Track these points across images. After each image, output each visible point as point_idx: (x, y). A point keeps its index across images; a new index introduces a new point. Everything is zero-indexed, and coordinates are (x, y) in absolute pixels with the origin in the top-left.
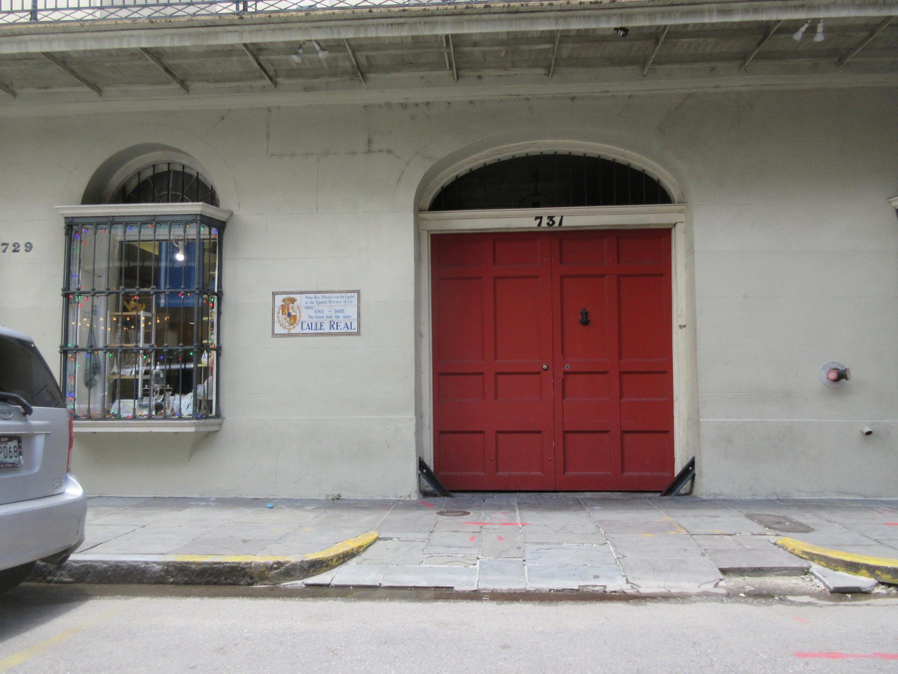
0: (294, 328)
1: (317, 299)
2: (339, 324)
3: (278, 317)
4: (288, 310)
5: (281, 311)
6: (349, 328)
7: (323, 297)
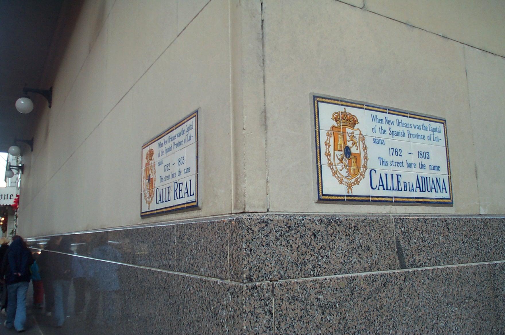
0: (357, 182)
1: (391, 126)
3: (328, 155)
7: (399, 124)
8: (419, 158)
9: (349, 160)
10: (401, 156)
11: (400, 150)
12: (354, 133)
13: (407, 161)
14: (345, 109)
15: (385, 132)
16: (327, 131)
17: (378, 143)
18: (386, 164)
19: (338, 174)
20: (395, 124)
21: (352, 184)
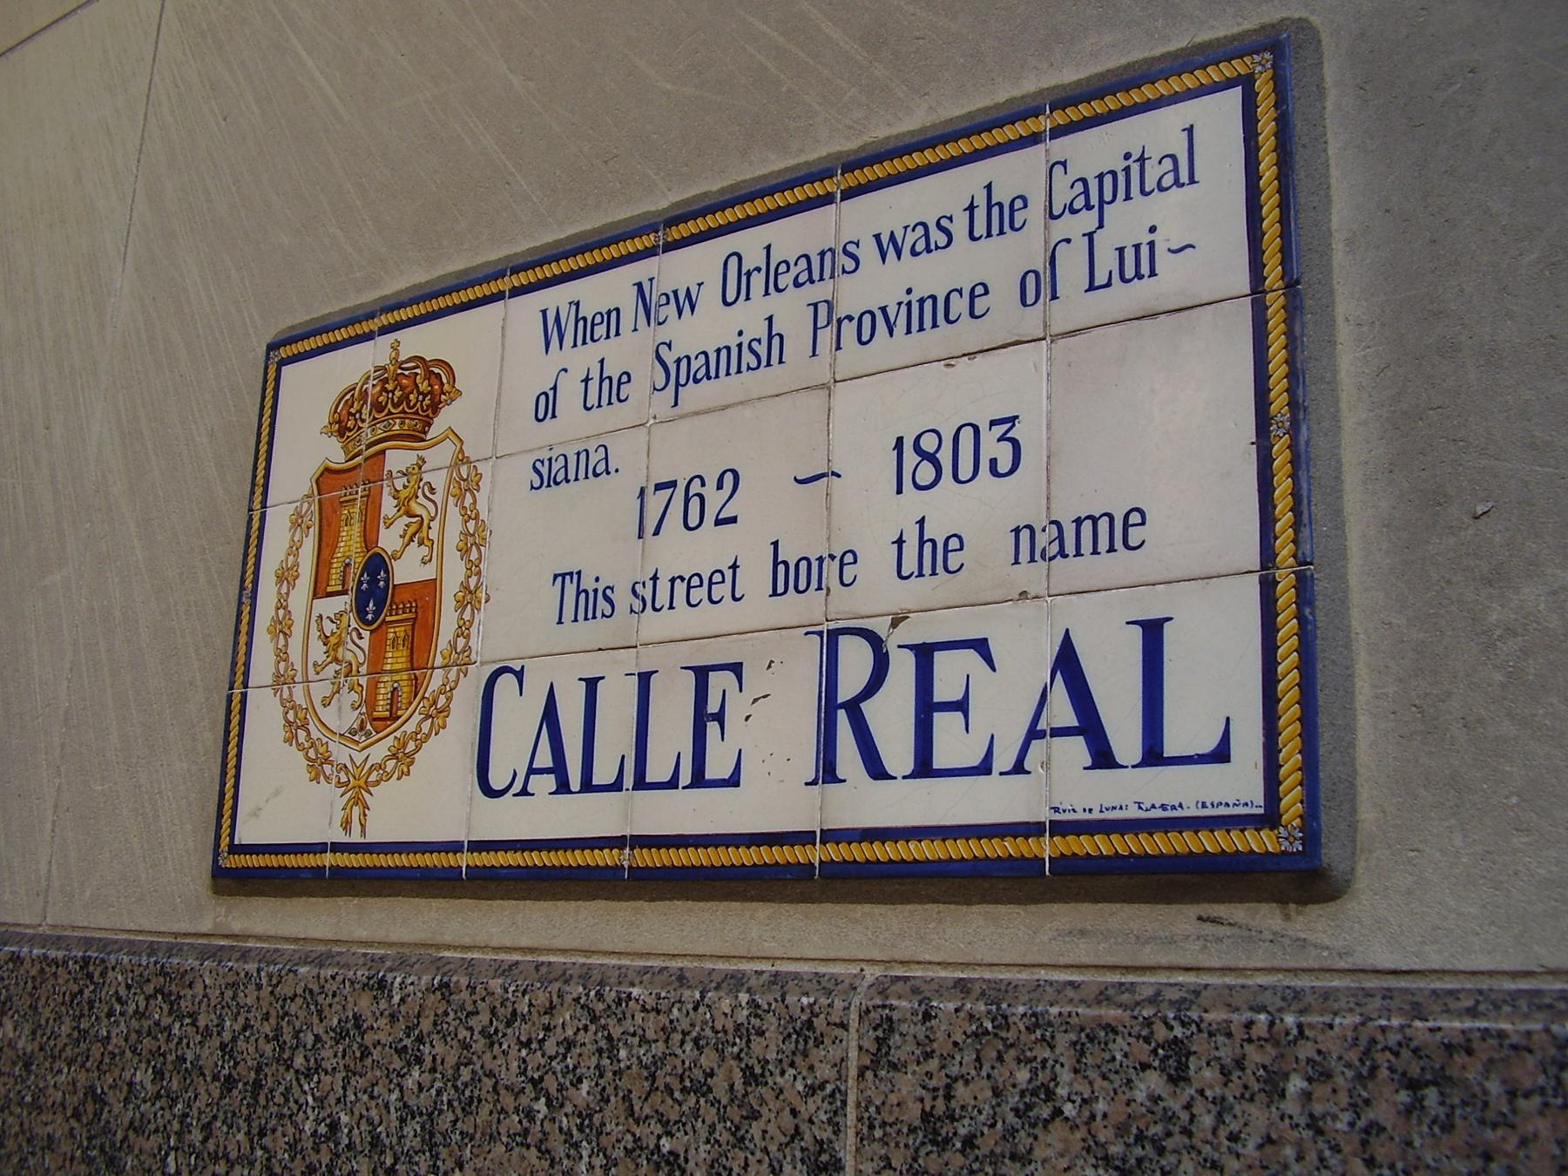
3: (282, 628)
4: (369, 539)
6: (1126, 738)
8: (899, 491)
10: (733, 520)
11: (729, 477)
13: (776, 544)
19: (311, 727)
21: (373, 777)
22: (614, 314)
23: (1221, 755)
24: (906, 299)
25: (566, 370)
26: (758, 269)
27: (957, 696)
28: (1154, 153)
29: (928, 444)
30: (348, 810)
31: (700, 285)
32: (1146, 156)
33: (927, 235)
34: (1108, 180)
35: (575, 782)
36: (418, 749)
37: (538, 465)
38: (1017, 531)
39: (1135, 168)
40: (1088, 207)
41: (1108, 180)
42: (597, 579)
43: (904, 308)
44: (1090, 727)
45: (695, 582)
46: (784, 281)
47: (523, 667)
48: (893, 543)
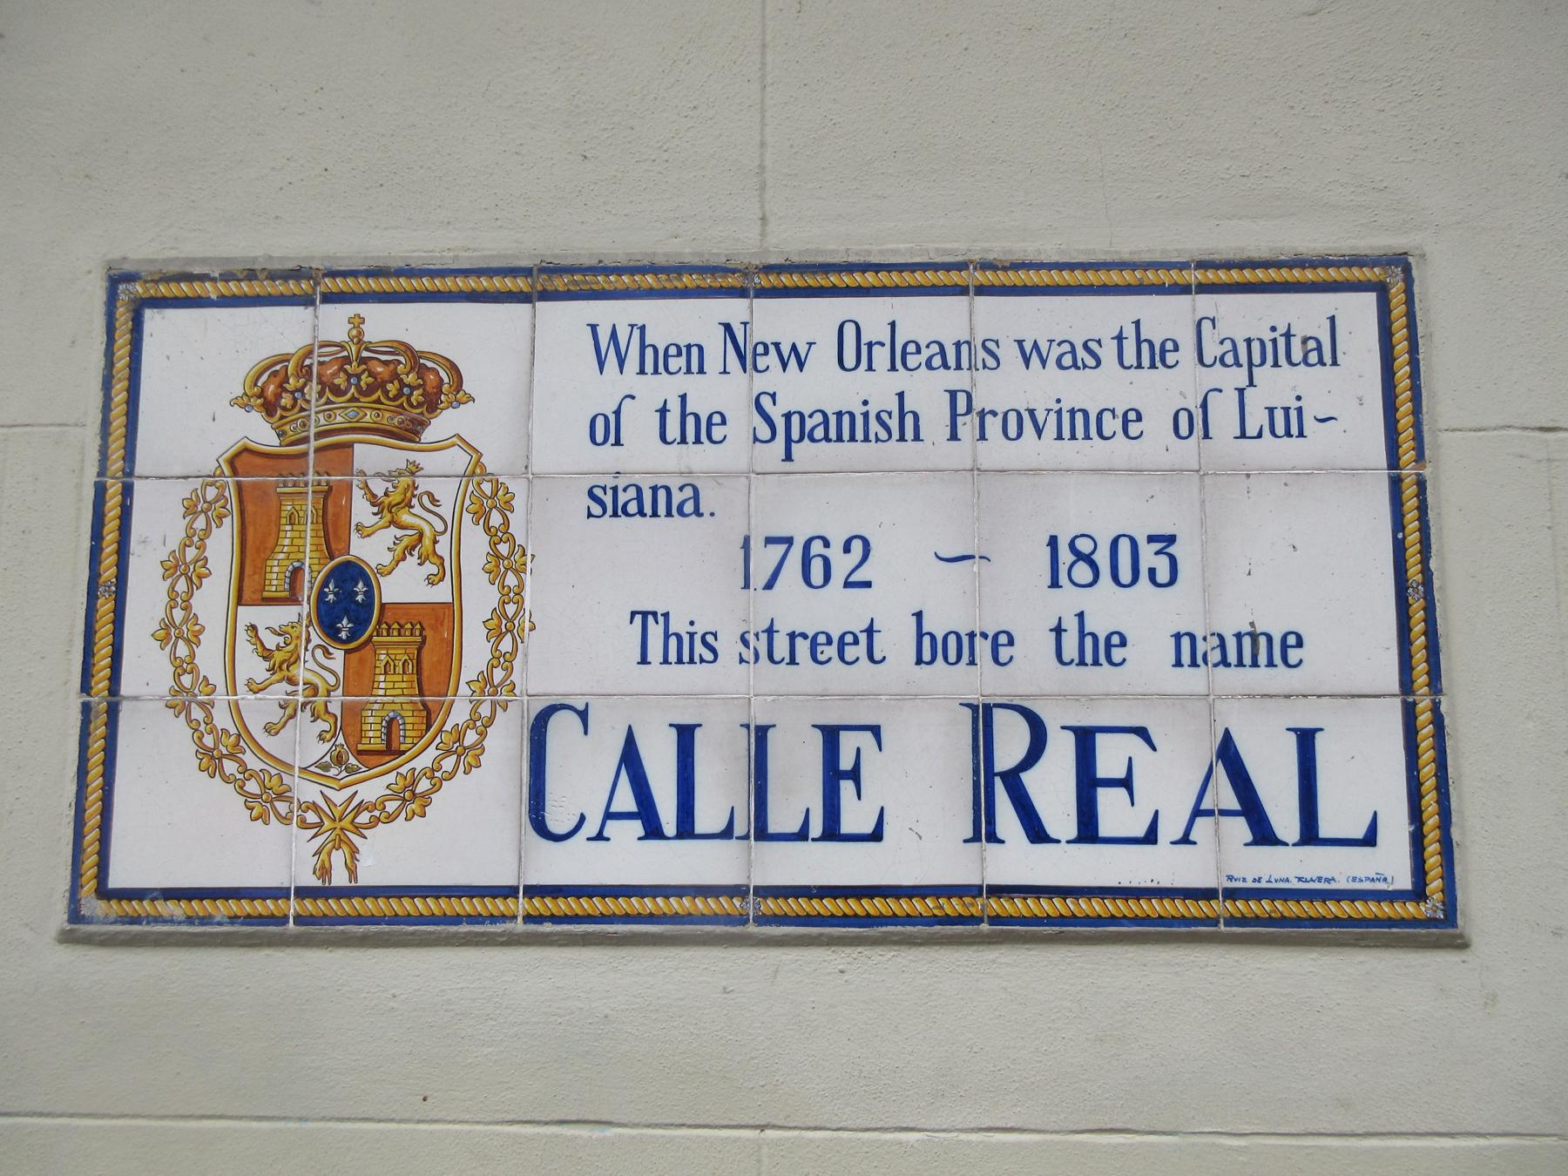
0: (412, 799)
1: (773, 378)
2: (1110, 757)
5: (221, 547)
6: (1285, 821)
8: (1055, 584)
9: (347, 652)
10: (868, 584)
11: (857, 546)
12: (413, 470)
13: (919, 615)
14: (357, 322)
15: (717, 433)
16: (184, 489)
17: (641, 513)
18: (699, 649)
20: (823, 357)
21: (364, 818)
22: (695, 351)
23: (1370, 839)
24: (1056, 407)
25: (633, 397)
26: (883, 345)
27: (1121, 773)
28: (1299, 332)
29: (1084, 546)
30: (324, 856)
31: (810, 344)
32: (1292, 333)
33: (1073, 351)
34: (1256, 346)
35: (670, 827)
36: (436, 788)
37: (598, 492)
38: (1178, 637)
39: (1281, 342)
40: (1240, 365)
41: (1256, 346)
42: (692, 623)
43: (1053, 417)
44: (1251, 808)
45: (822, 639)
46: (912, 361)
47: (587, 705)
48: (1051, 630)
